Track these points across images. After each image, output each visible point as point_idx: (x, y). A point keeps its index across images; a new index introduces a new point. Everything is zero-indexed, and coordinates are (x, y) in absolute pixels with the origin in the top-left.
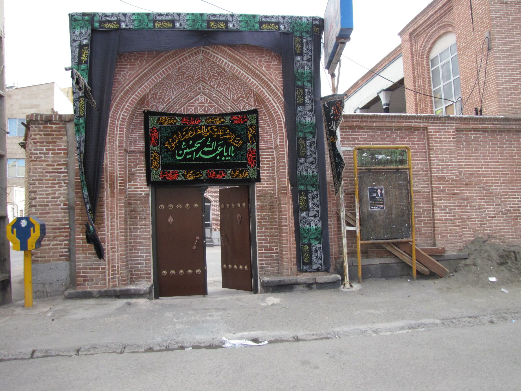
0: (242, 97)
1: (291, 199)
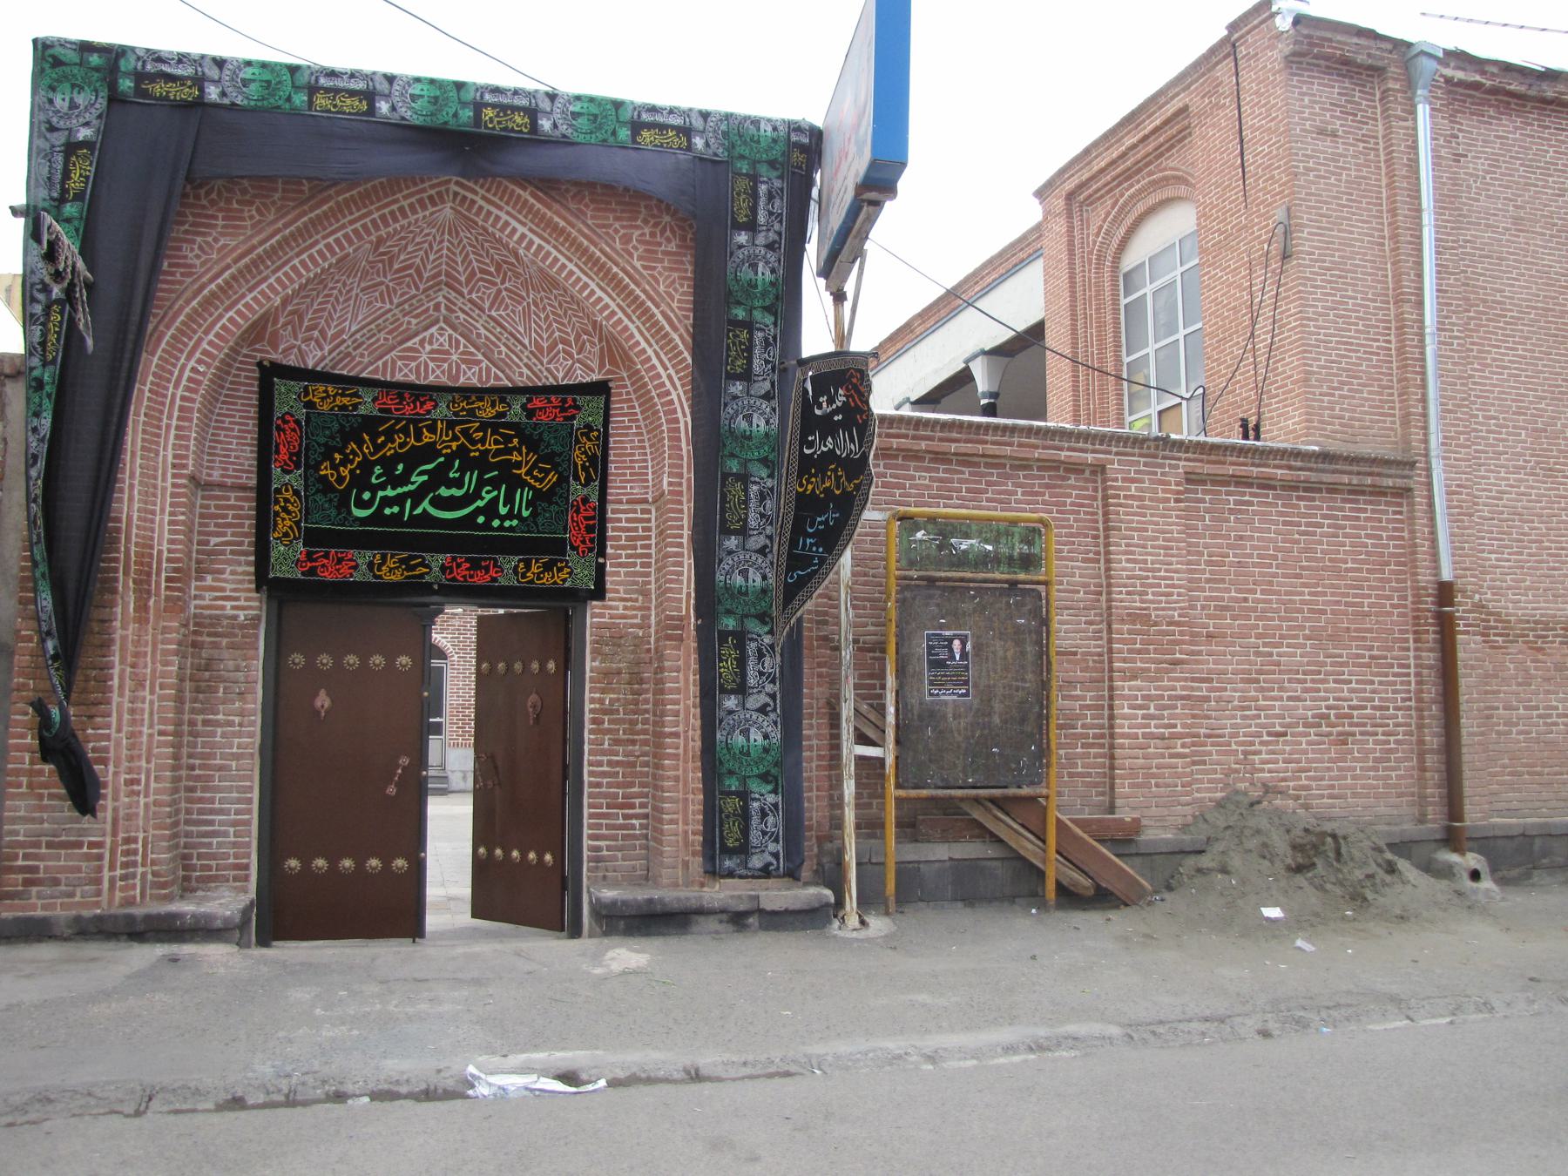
0: (565, 342)
1: (694, 657)
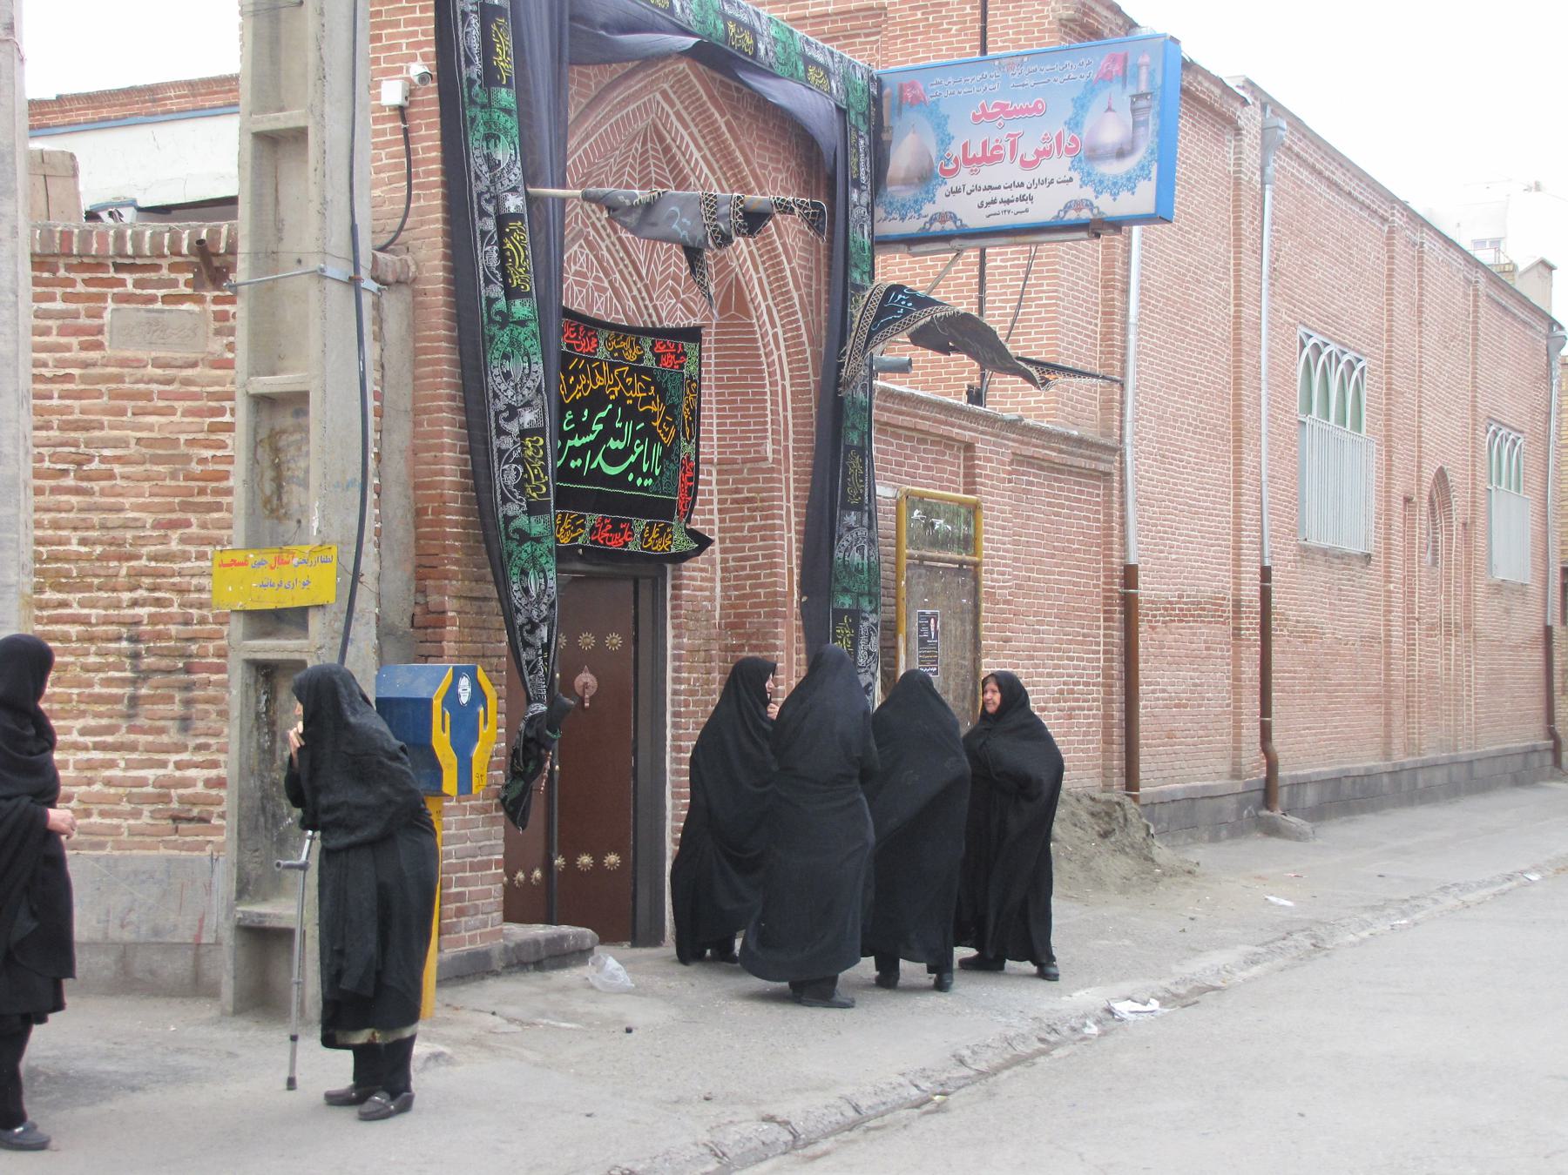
0: (676, 279)
